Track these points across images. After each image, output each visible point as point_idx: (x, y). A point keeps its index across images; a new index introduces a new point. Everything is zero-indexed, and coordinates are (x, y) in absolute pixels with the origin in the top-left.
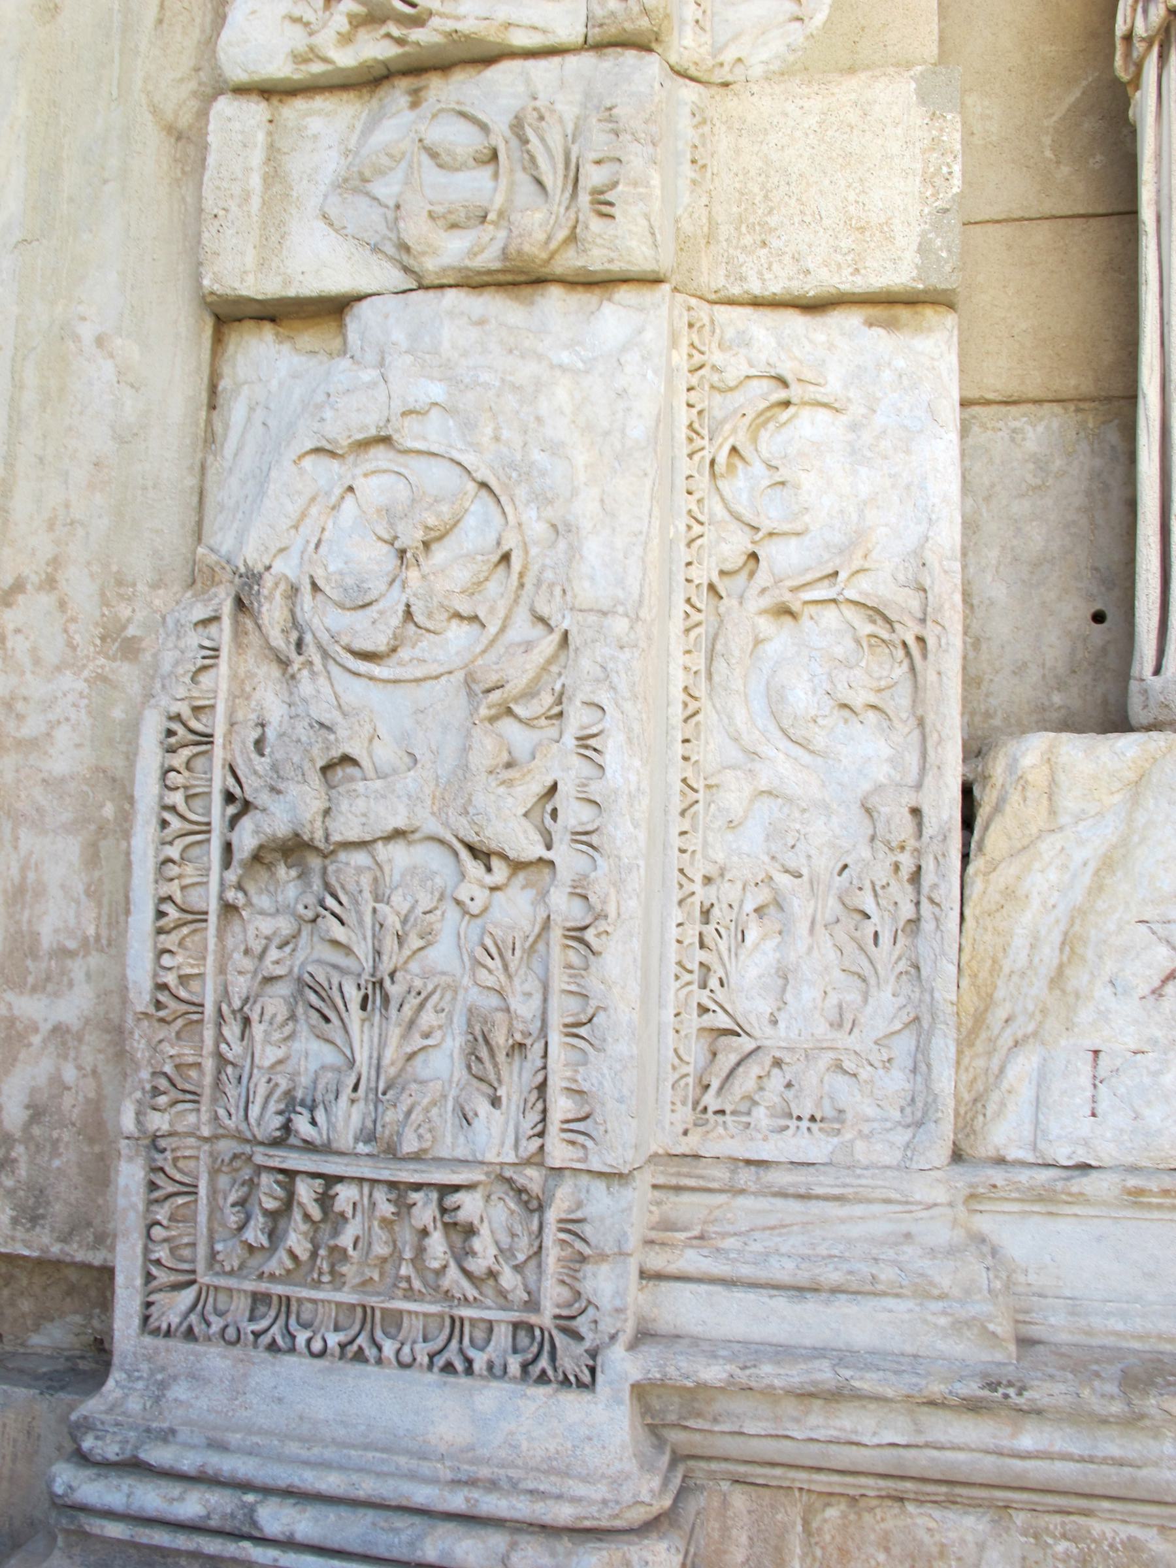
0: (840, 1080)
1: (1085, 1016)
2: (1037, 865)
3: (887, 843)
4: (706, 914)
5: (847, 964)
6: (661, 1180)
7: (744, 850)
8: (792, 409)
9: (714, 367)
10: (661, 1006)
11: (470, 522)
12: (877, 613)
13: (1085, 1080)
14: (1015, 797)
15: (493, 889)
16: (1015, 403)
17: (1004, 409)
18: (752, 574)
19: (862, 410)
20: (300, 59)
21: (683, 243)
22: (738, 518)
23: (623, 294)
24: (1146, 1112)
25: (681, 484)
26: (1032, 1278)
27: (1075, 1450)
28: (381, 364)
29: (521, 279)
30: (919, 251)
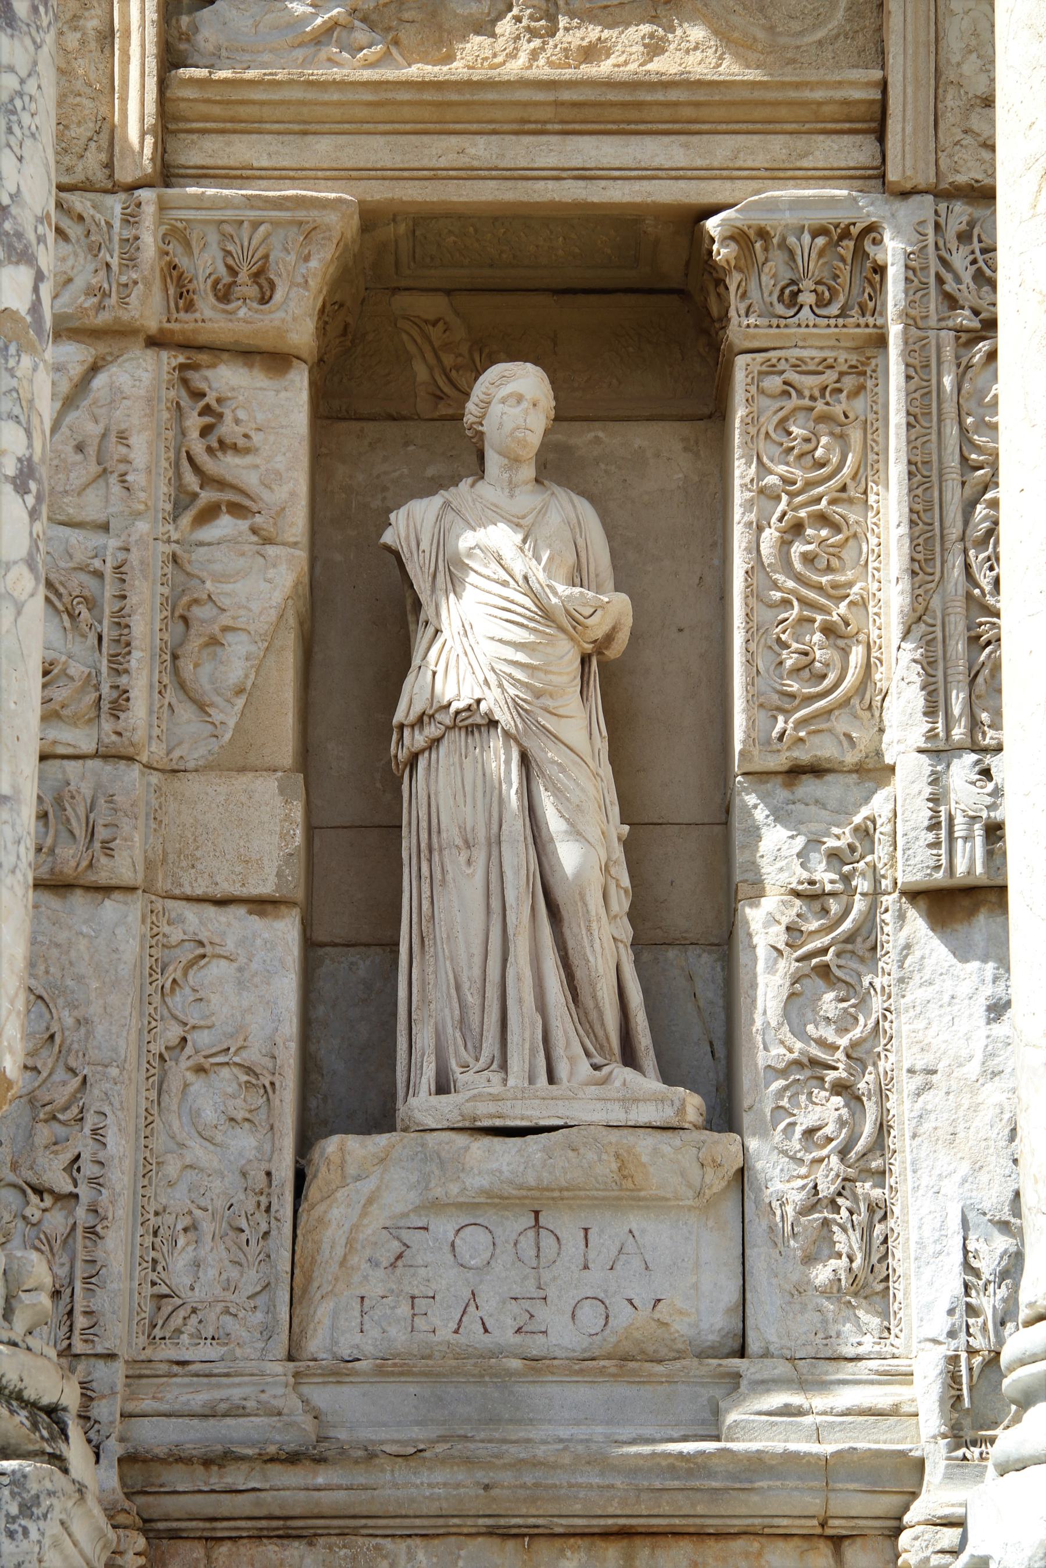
0: (228, 1318)
1: (356, 1278)
3: (253, 1190)
4: (155, 1234)
5: (232, 1258)
6: (130, 1373)
7: (178, 1199)
8: (206, 960)
9: (164, 935)
10: (132, 1279)
12: (249, 1070)
13: (357, 1314)
14: (323, 1169)
15: (44, 1211)
17: (346, 949)
18: (183, 1049)
22: (175, 1017)
23: (116, 895)
24: (388, 1329)
25: (146, 999)
26: (329, 1418)
27: (344, 1482)
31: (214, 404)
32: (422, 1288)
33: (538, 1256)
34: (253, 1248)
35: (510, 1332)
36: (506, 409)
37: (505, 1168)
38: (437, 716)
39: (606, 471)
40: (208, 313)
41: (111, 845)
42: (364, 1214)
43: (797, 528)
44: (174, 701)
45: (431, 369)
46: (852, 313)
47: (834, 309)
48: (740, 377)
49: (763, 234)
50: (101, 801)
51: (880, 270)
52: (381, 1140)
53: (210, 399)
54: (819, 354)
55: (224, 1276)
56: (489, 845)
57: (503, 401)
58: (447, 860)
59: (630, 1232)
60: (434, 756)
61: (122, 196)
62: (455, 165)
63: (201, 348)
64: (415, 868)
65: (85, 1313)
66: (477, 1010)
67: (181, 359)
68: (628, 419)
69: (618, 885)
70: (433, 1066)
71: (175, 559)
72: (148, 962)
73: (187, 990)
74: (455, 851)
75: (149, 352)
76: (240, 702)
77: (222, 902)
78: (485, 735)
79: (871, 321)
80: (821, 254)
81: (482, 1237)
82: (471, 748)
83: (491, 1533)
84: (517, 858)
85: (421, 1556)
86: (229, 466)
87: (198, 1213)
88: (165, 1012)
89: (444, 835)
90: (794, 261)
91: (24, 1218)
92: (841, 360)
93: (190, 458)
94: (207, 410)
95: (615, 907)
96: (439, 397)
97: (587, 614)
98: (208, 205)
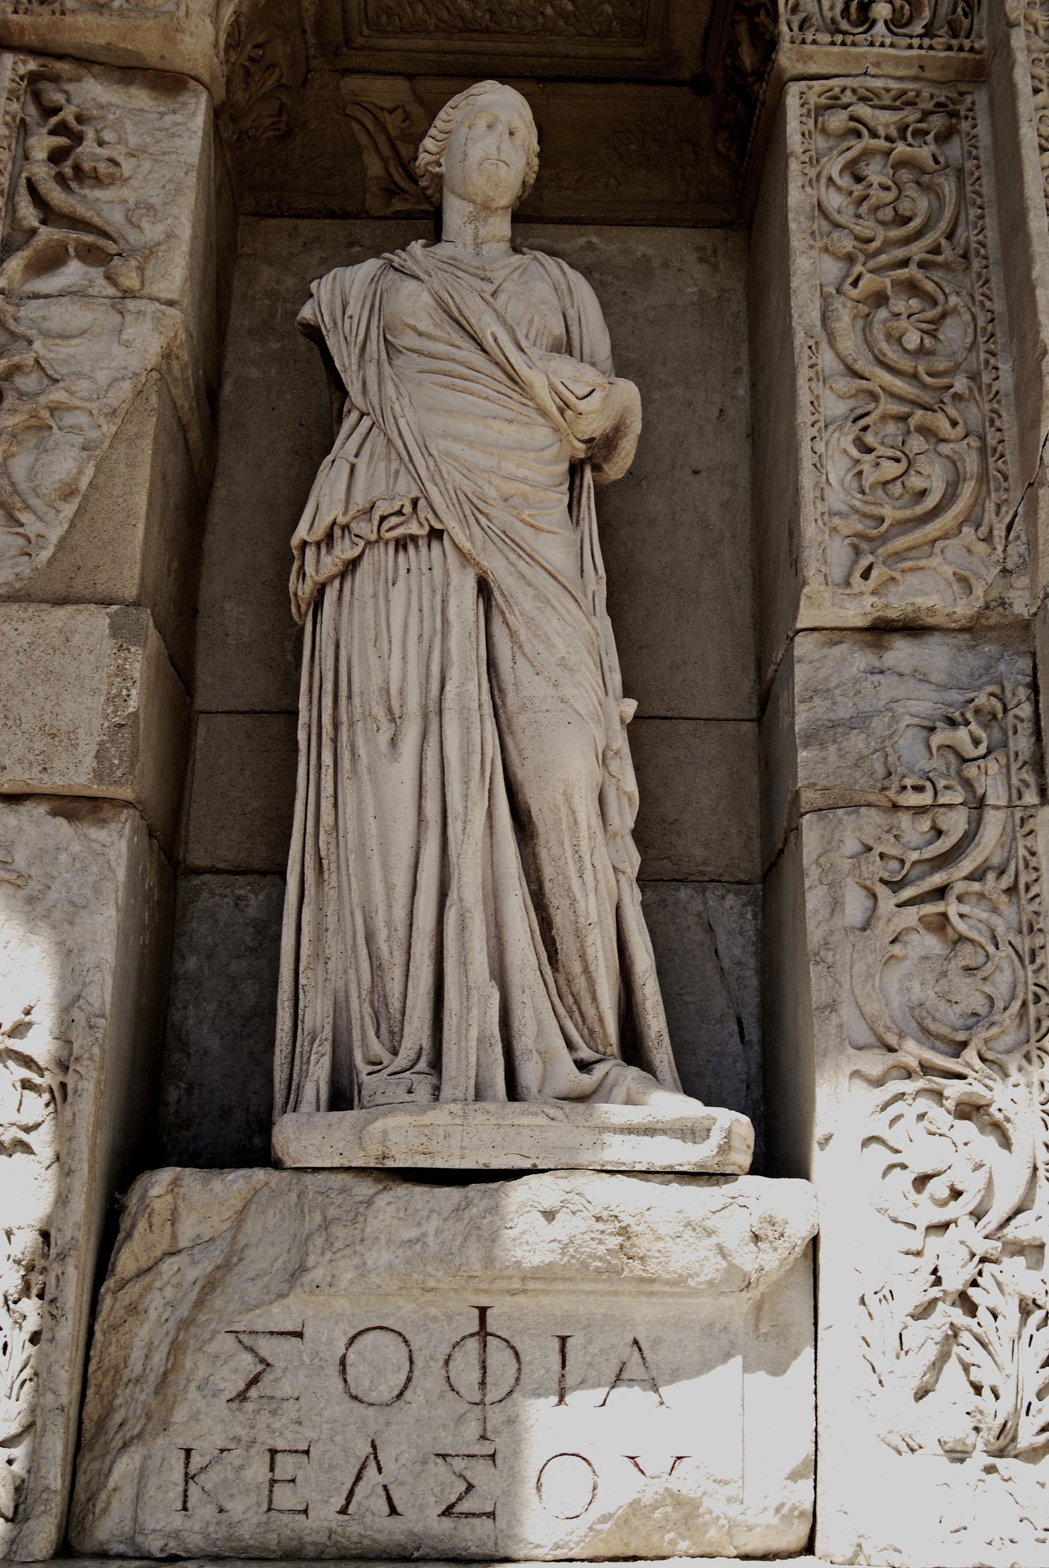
2: (158, 1284)
13: (178, 1475)
16: (243, 873)
17: (232, 878)
19: (39, 887)
24: (228, 1505)
30: (96, 757)
33: (483, 1383)
38: (353, 525)
39: (601, 282)
45: (385, 161)
46: (939, 33)
52: (238, 1182)
53: (68, 114)
56: (425, 717)
58: (360, 741)
59: (636, 1342)
60: (347, 585)
63: (60, 57)
66: (398, 973)
67: (32, 65)
68: (628, 223)
70: (326, 1061)
76: (69, 509)
78: (424, 549)
82: (402, 570)
84: (468, 733)
89: (356, 701)
92: (926, 94)
94: (61, 129)
96: (392, 191)
97: (581, 394)
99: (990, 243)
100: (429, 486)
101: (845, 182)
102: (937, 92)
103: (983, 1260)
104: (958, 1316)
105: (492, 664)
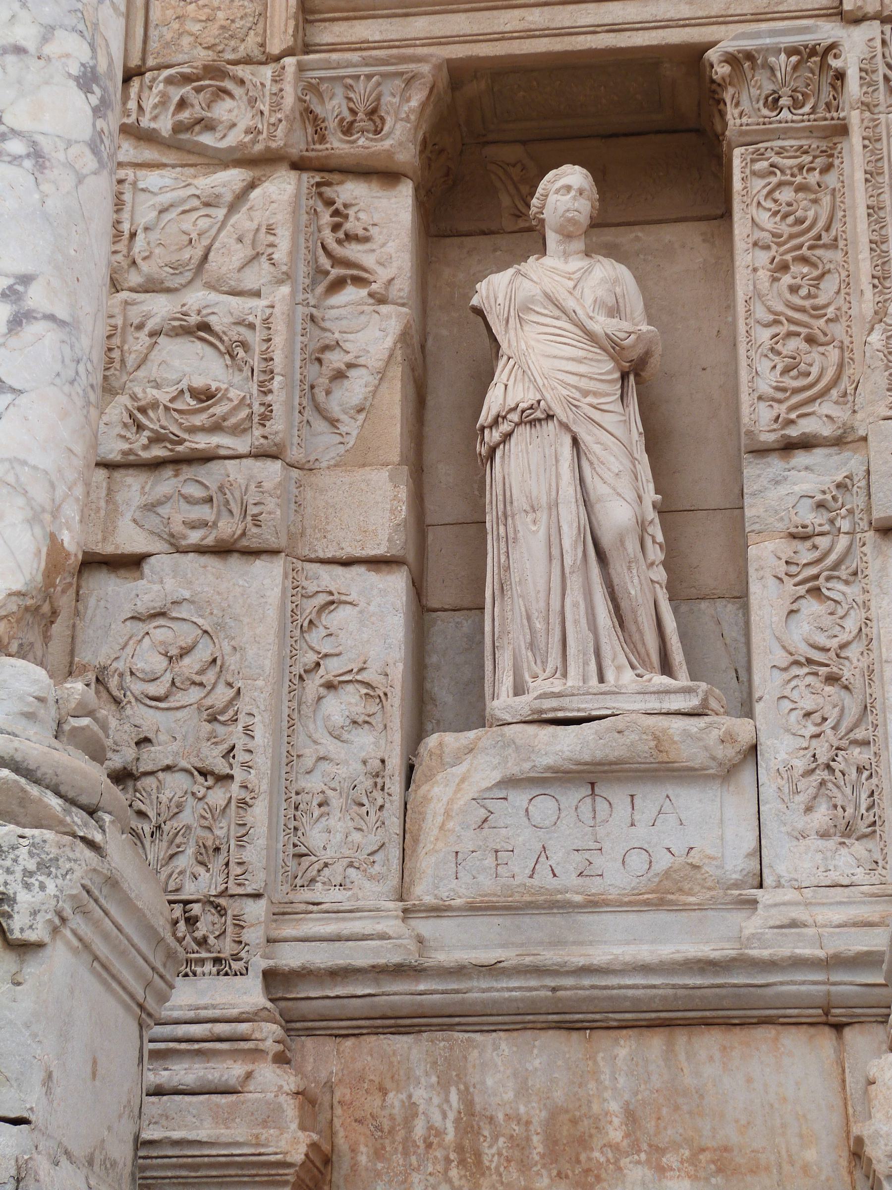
4: (296, 808)
6: (276, 910)
7: (314, 783)
10: (277, 841)
11: (200, 646)
12: (367, 685)
13: (454, 865)
15: (208, 788)
20: (125, 453)
21: (291, 536)
22: (312, 649)
23: (264, 557)
25: (288, 634)
26: (432, 944)
28: (162, 582)
29: (222, 550)
31: (341, 208)
32: (503, 844)
34: (373, 817)
35: (574, 876)
36: (559, 197)
37: (566, 749)
40: (336, 144)
41: (260, 518)
42: (458, 790)
43: (784, 267)
44: (310, 419)
47: (807, 109)
48: (737, 163)
49: (749, 56)
50: (252, 487)
51: (840, 76)
53: (338, 205)
54: (795, 143)
55: (350, 839)
56: (550, 508)
57: (557, 192)
58: (518, 523)
59: (668, 796)
60: (507, 447)
61: (273, 65)
62: (517, 28)
63: (331, 171)
64: (495, 533)
65: (239, 864)
67: (318, 179)
69: (654, 542)
70: (511, 678)
71: (312, 318)
72: (290, 607)
73: (321, 628)
74: (523, 514)
75: (293, 174)
77: (347, 563)
79: (835, 115)
80: (795, 68)
81: (550, 804)
82: (534, 436)
83: (559, 1026)
84: (570, 516)
85: (503, 1046)
86: (352, 251)
87: (330, 793)
88: (305, 646)
89: (515, 504)
90: (775, 76)
91: (193, 794)
92: (814, 146)
93: (324, 247)
94: (336, 213)
95: (651, 556)
98: (335, 65)
99: (848, 231)
100: (545, 393)
101: (769, 204)
102: (821, 144)
103: (838, 749)
104: (825, 775)
105: (582, 480)
